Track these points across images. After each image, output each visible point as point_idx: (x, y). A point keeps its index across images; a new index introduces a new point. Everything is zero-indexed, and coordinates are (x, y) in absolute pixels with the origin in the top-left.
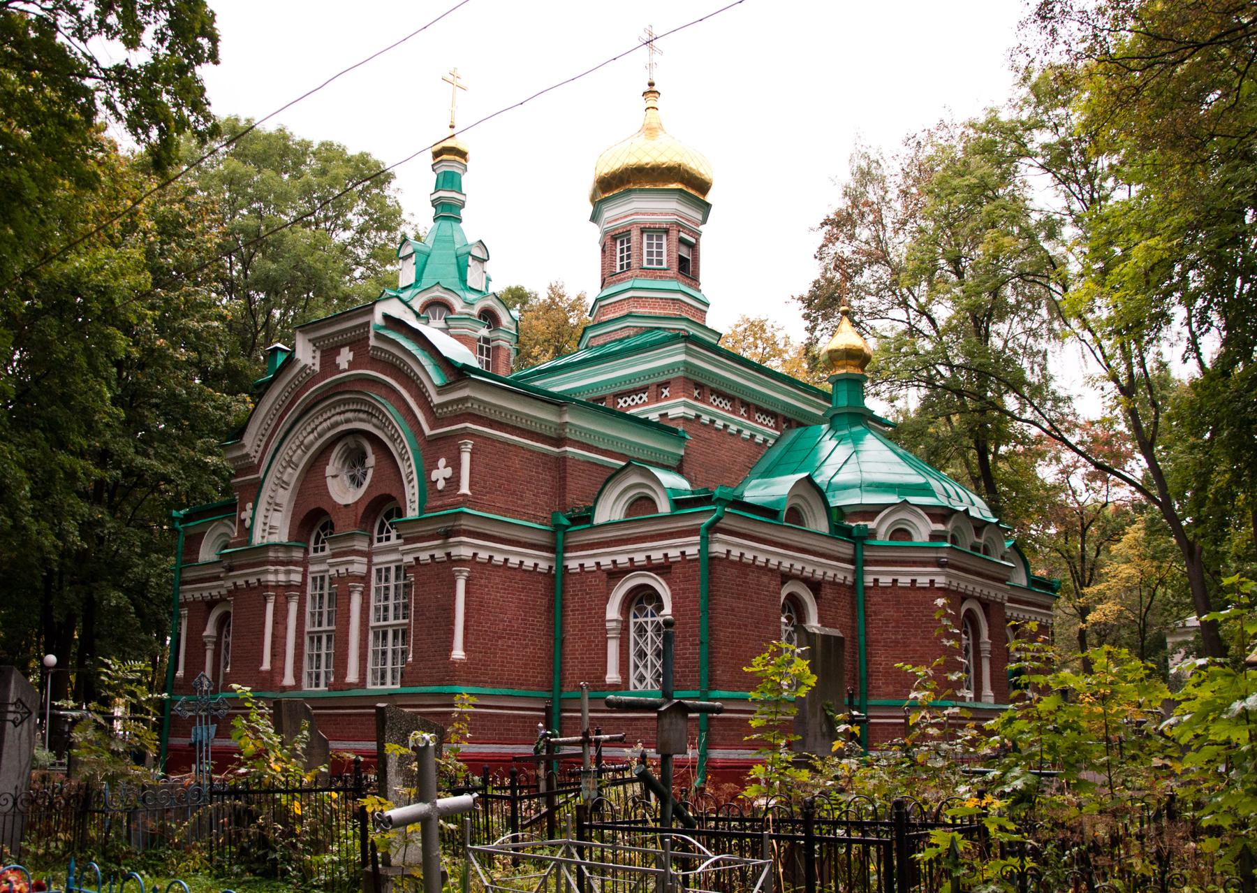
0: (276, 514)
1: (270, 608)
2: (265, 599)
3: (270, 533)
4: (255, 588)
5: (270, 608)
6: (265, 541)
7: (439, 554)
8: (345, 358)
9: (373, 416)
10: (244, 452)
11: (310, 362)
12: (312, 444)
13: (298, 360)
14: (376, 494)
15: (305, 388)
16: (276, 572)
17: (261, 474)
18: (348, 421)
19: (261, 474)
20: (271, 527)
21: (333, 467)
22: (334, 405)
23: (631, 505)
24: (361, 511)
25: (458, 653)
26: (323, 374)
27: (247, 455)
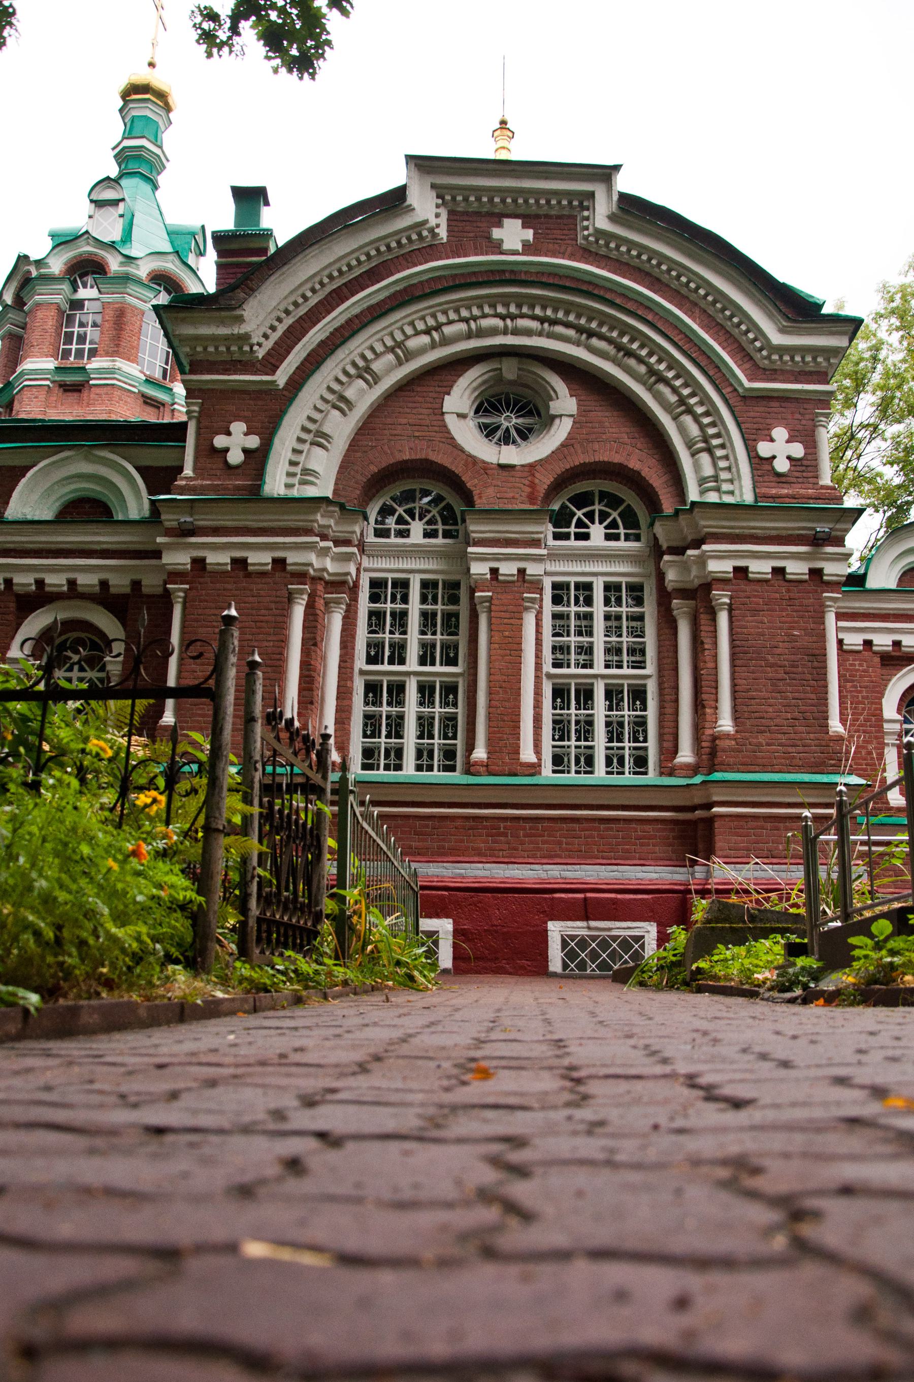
0: (317, 450)
1: (298, 613)
2: (290, 599)
3: (303, 483)
4: (263, 574)
5: (298, 613)
6: (295, 493)
7: (797, 569)
8: (513, 235)
9: (591, 334)
10: (243, 329)
11: (433, 222)
12: (422, 351)
13: (410, 209)
14: (581, 458)
15: (409, 259)
16: (324, 552)
17: (281, 377)
18: (516, 332)
19: (281, 377)
20: (306, 471)
21: (459, 398)
22: (493, 301)
23: (904, 574)
24: (545, 480)
25: (835, 725)
26: (455, 247)
27: (246, 337)
